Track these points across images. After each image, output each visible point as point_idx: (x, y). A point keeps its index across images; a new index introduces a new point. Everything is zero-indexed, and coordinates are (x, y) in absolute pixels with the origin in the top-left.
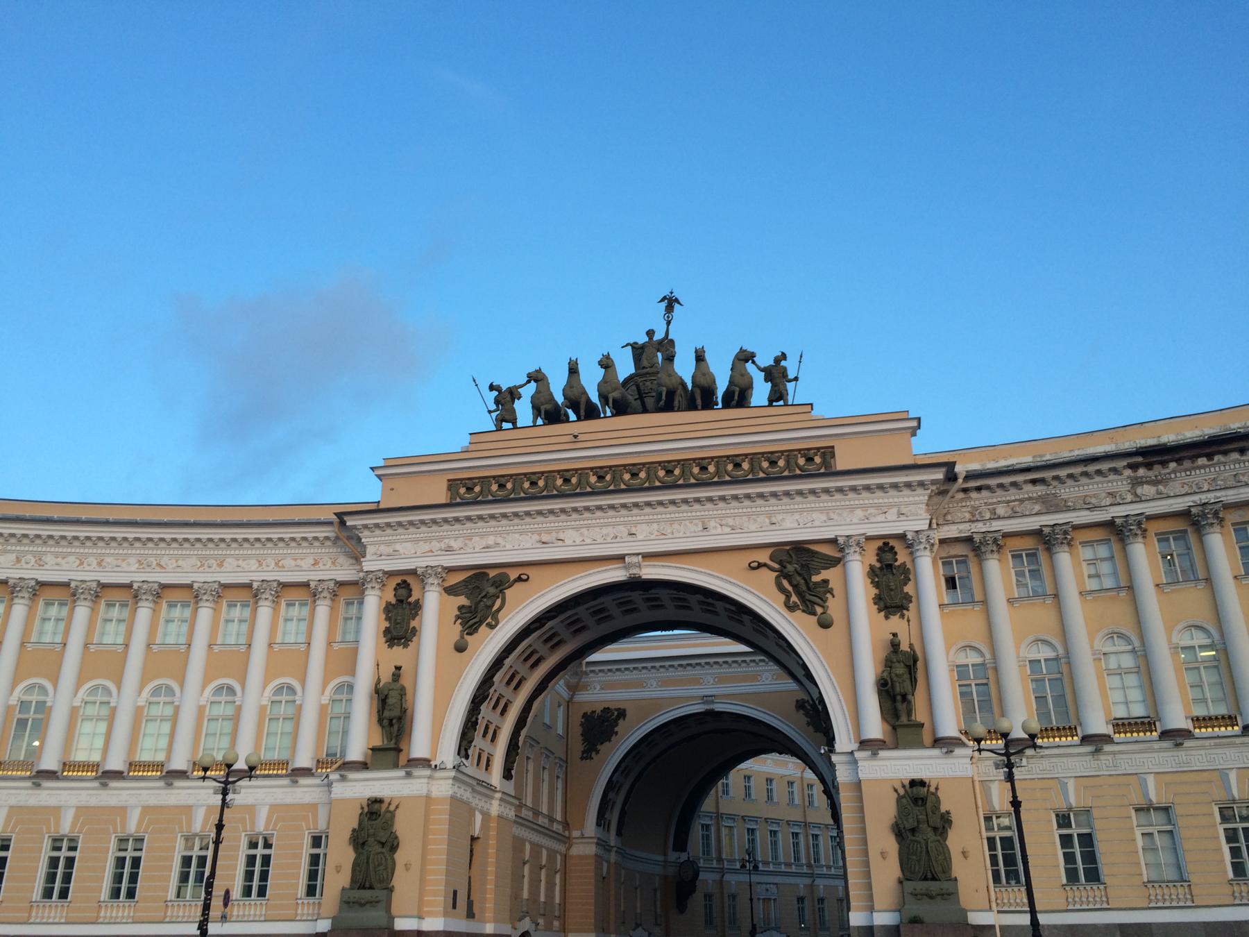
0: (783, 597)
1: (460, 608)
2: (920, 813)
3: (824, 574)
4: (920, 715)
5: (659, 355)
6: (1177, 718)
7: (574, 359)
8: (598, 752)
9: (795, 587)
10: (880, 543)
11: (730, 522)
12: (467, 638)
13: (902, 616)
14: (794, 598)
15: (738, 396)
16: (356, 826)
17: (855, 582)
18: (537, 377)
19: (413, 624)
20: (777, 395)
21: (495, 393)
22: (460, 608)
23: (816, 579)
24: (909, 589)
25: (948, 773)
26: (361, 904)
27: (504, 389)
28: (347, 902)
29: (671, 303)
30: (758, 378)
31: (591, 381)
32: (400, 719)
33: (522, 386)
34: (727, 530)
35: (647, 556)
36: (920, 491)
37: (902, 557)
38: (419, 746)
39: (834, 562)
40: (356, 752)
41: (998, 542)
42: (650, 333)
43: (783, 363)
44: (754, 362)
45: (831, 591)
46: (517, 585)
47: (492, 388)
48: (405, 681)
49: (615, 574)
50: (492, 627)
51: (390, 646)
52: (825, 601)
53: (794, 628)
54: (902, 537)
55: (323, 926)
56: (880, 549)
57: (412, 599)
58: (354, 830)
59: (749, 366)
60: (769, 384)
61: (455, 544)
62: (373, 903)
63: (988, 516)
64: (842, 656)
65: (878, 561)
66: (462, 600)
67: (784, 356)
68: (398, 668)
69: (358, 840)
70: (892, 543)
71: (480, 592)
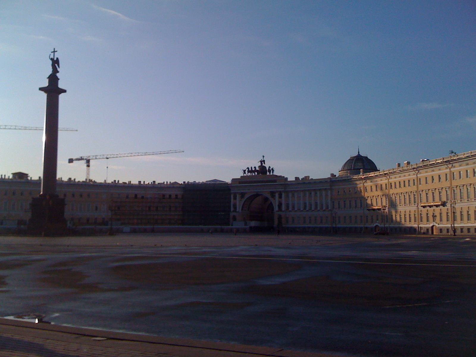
2: (280, 218)
6: (302, 209)
15: (269, 171)
17: (277, 195)
18: (248, 168)
20: (273, 172)
29: (263, 157)
31: (253, 169)
38: (237, 210)
39: (275, 193)
41: (291, 191)
47: (243, 170)
49: (256, 193)
53: (271, 199)
64: (276, 203)
71: (243, 195)
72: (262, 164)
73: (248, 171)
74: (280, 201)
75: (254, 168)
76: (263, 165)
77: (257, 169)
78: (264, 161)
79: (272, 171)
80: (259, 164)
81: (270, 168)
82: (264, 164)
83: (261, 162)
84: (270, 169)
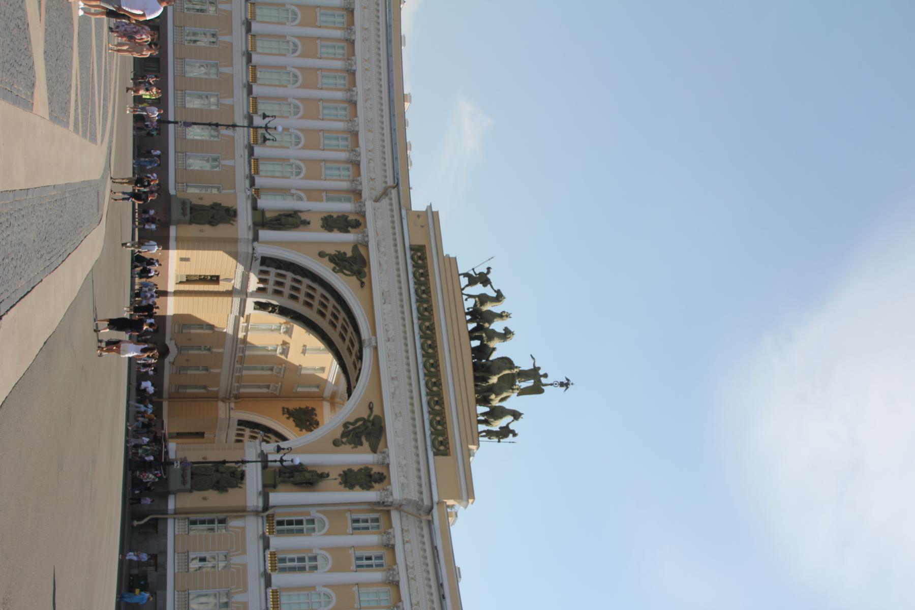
0: (352, 420)
1: (345, 253)
2: (226, 476)
3: (366, 444)
4: (280, 487)
8: (288, 418)
9: (358, 427)
10: (385, 474)
12: (327, 258)
13: (340, 483)
14: (351, 427)
16: (223, 205)
17: (361, 457)
18: (499, 297)
19: (335, 230)
21: (485, 271)
22: (345, 253)
24: (357, 487)
25: (248, 492)
26: (184, 209)
28: (184, 203)
29: (565, 385)
31: (498, 326)
32: (280, 224)
34: (393, 390)
35: (376, 348)
36: (418, 495)
37: (376, 485)
38: (264, 234)
39: (374, 451)
40: (262, 203)
42: (545, 376)
43: (511, 435)
45: (356, 447)
46: (358, 283)
47: (489, 269)
48: (301, 227)
50: (334, 270)
51: (322, 219)
52: (350, 443)
55: (172, 192)
57: (350, 229)
58: (220, 204)
61: (382, 249)
62: (184, 214)
63: (406, 539)
66: (349, 254)
67: (515, 435)
68: (309, 223)
69: (216, 206)
70: (386, 482)
71: (354, 264)
72: (525, 375)
74: (323, 476)
75: (506, 329)
77: (500, 349)
78: (537, 389)
79: (496, 426)
80: (524, 364)
81: (509, 418)
83: (534, 374)
84: (508, 419)
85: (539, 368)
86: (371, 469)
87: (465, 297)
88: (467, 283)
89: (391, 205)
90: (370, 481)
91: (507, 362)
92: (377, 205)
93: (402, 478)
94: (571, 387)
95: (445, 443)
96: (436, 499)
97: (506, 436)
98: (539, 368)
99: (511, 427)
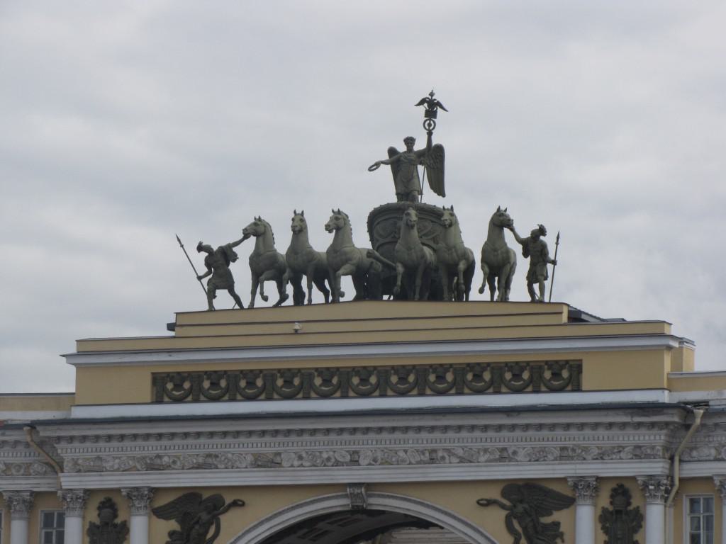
3: (557, 516)
5: (421, 169)
7: (299, 212)
9: (525, 529)
10: (614, 485)
11: (460, 452)
18: (259, 230)
20: (536, 276)
21: (204, 254)
23: (546, 520)
27: (215, 248)
29: (432, 107)
30: (517, 249)
31: (320, 241)
33: (237, 244)
34: (455, 460)
36: (655, 431)
37: (636, 502)
39: (568, 502)
42: (410, 142)
43: (542, 238)
44: (512, 230)
45: (561, 535)
54: (633, 479)
56: (614, 490)
57: (118, 521)
59: (506, 231)
60: (529, 258)
65: (611, 503)
66: (173, 525)
67: (542, 231)
70: (627, 485)
73: (254, 261)
76: (429, 197)
79: (523, 265)
82: (439, 188)
83: (401, 163)
85: (392, 152)
86: (604, 510)
87: (259, 303)
88: (226, 292)
89: (71, 439)
90: (627, 513)
91: (378, 218)
92: (67, 465)
93: (622, 455)
94: (437, 97)
95: (556, 367)
96: (665, 397)
97: (543, 247)
98: (392, 152)
99: (525, 234)
